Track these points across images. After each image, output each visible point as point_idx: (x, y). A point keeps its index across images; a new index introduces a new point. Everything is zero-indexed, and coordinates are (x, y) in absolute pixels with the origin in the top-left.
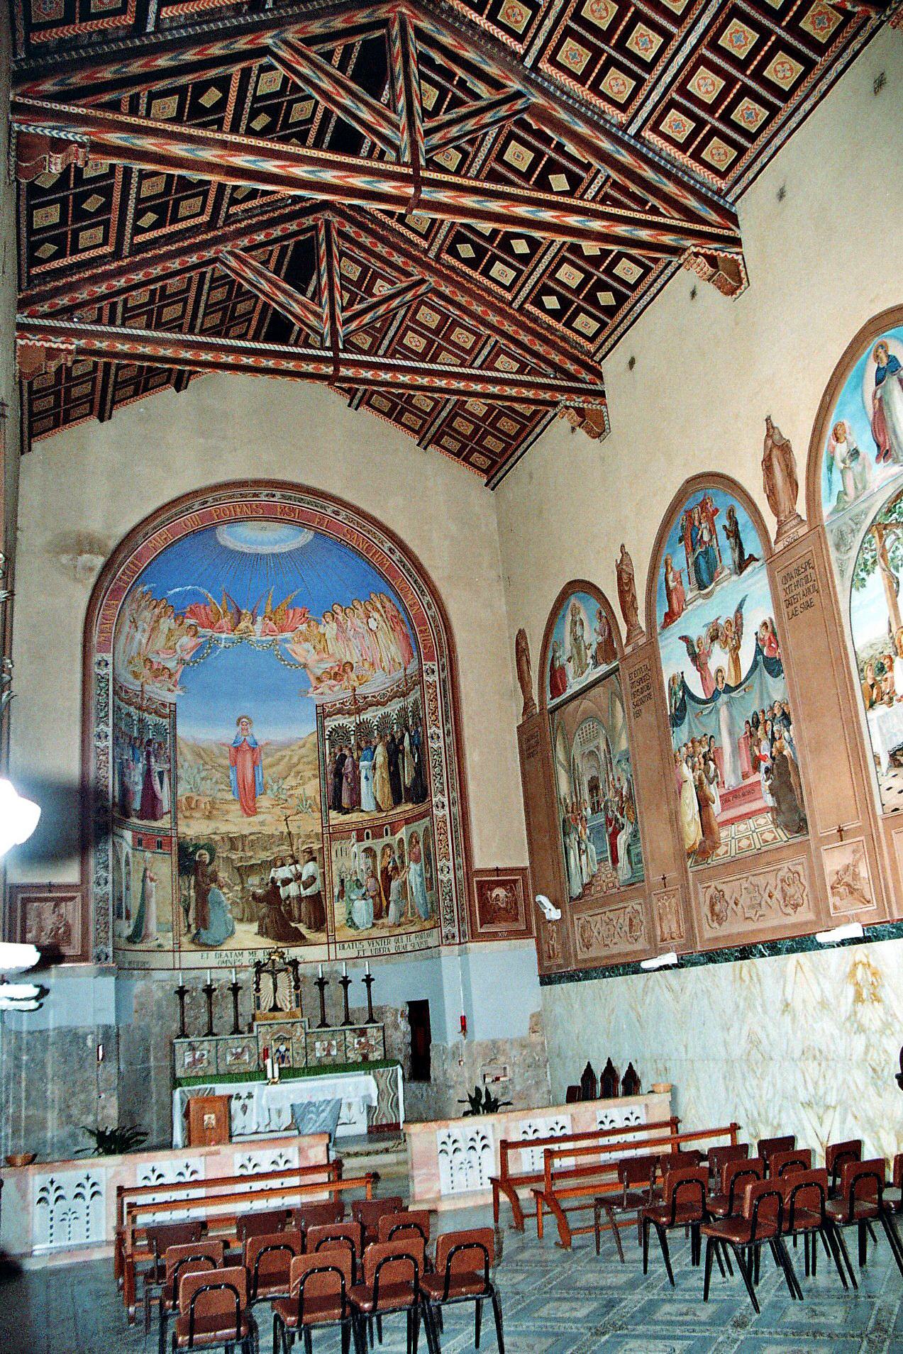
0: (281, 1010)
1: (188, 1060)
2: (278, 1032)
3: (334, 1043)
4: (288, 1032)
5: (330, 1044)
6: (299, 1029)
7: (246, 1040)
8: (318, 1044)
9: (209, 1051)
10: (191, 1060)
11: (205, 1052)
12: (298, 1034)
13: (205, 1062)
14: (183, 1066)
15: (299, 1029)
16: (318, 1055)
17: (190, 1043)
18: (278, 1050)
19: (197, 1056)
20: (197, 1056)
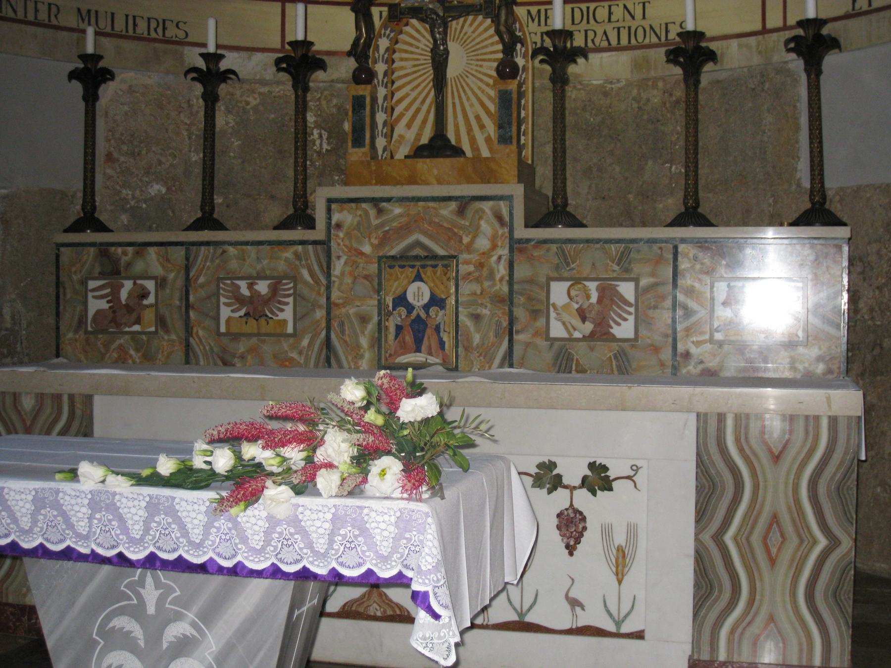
0: (457, 152)
1: (96, 305)
2: (404, 230)
3: (627, 290)
4: (450, 234)
5: (608, 295)
6: (486, 227)
7: (288, 254)
8: (559, 292)
9: (161, 283)
10: (103, 305)
11: (150, 285)
12: (483, 243)
13: (149, 316)
14: (82, 321)
15: (486, 227)
16: (557, 330)
17: (104, 250)
18: (401, 300)
19: (124, 295)
20: (124, 295)
